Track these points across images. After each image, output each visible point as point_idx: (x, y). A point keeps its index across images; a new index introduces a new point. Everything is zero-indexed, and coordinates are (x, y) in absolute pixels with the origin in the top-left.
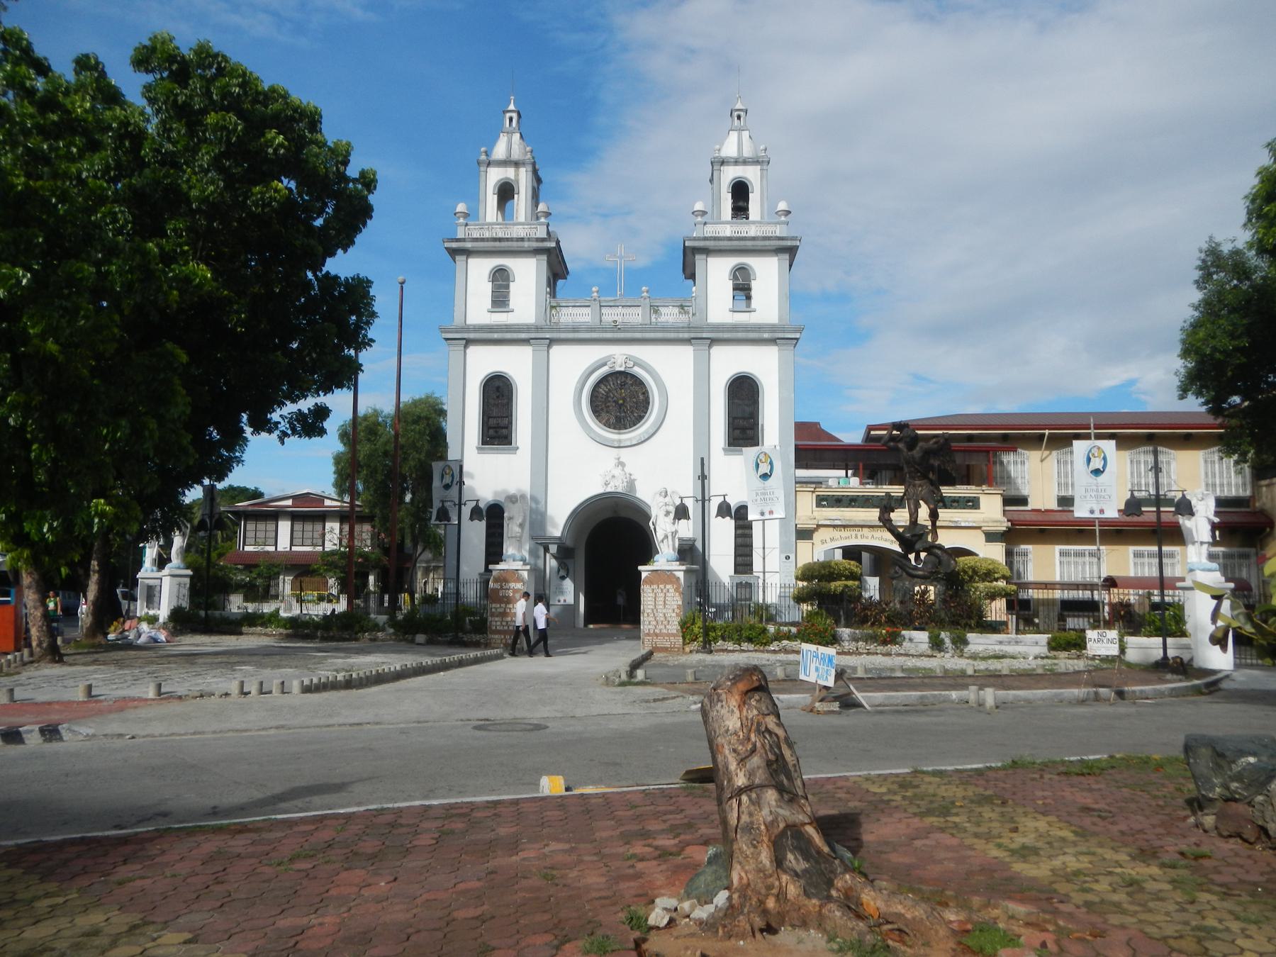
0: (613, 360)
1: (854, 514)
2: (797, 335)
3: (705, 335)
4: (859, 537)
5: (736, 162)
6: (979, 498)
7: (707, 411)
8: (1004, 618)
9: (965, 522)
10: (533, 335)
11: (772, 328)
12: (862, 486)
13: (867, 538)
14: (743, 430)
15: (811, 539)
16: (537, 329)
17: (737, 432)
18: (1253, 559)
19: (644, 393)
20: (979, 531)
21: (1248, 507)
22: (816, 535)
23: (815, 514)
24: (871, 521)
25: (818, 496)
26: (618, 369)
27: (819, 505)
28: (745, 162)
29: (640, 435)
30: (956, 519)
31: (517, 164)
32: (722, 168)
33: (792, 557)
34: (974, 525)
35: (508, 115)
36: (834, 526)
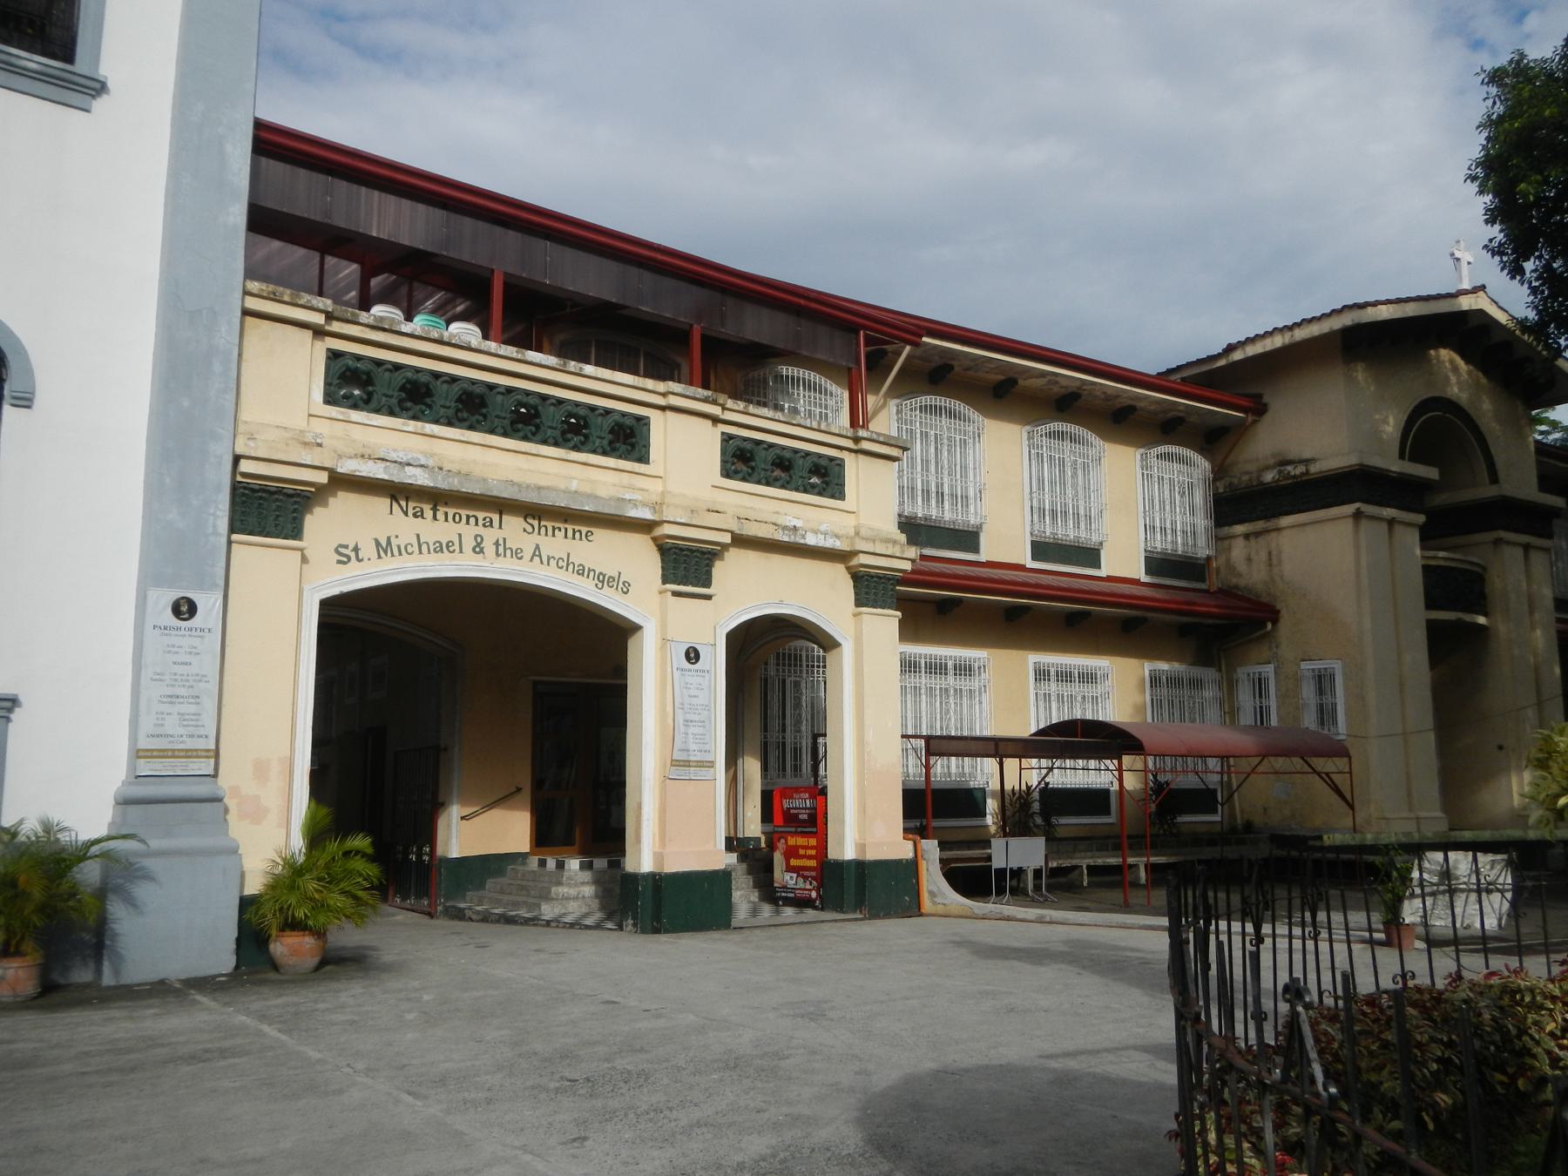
1: (474, 453)
4: (489, 547)
6: (840, 464)
8: (902, 850)
9: (816, 532)
12: (510, 351)
13: (517, 554)
15: (296, 533)
18: (1209, 693)
20: (839, 569)
21: (1203, 581)
22: (315, 521)
23: (322, 428)
24: (539, 488)
25: (334, 355)
27: (330, 399)
30: (791, 522)
33: (209, 604)
34: (838, 545)
36: (397, 492)
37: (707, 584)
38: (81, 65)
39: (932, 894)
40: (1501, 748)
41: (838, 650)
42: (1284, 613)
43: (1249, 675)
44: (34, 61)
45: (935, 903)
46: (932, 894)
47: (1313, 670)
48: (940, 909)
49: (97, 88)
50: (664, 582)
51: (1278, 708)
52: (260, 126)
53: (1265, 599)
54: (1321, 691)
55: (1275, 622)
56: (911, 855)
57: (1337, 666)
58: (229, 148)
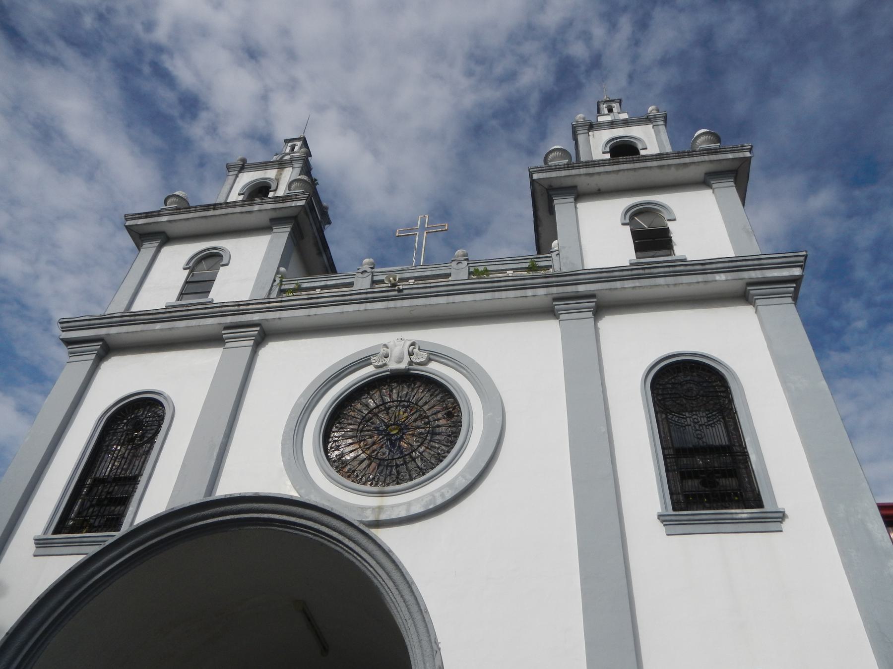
0: (382, 351)
2: (797, 272)
3: (582, 288)
5: (612, 124)
7: (604, 429)
10: (229, 320)
11: (732, 265)
14: (708, 477)
16: (239, 308)
17: (693, 484)
19: (449, 415)
26: (393, 366)
28: (626, 123)
29: (432, 494)
31: (281, 165)
32: (591, 133)
35: (290, 144)
38: (768, 507)
44: (744, 513)
49: (781, 517)
52: (882, 507)
58: (870, 526)
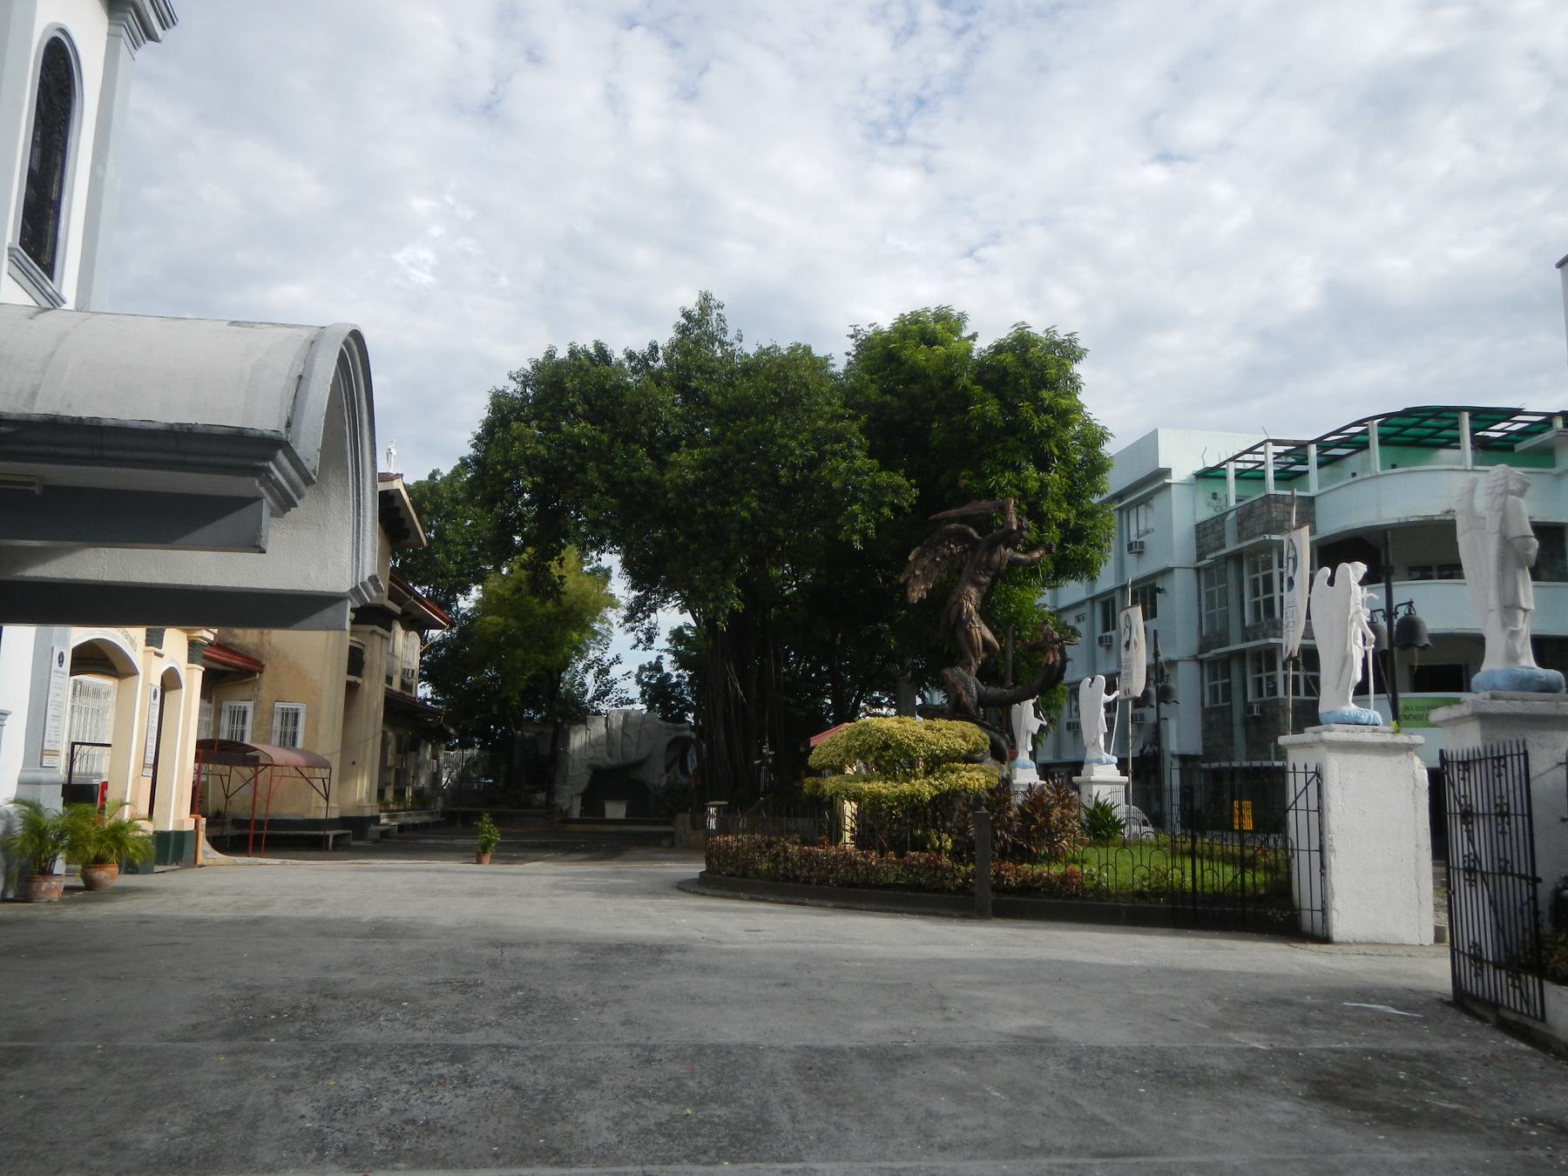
8: (189, 825)
37: (160, 646)
39: (205, 853)
40: (354, 763)
41: (178, 691)
42: (268, 668)
43: (230, 707)
45: (206, 858)
46: (205, 853)
47: (283, 709)
48: (210, 862)
50: (147, 645)
51: (253, 732)
53: (253, 656)
54: (284, 723)
55: (261, 672)
56: (192, 828)
57: (303, 709)
